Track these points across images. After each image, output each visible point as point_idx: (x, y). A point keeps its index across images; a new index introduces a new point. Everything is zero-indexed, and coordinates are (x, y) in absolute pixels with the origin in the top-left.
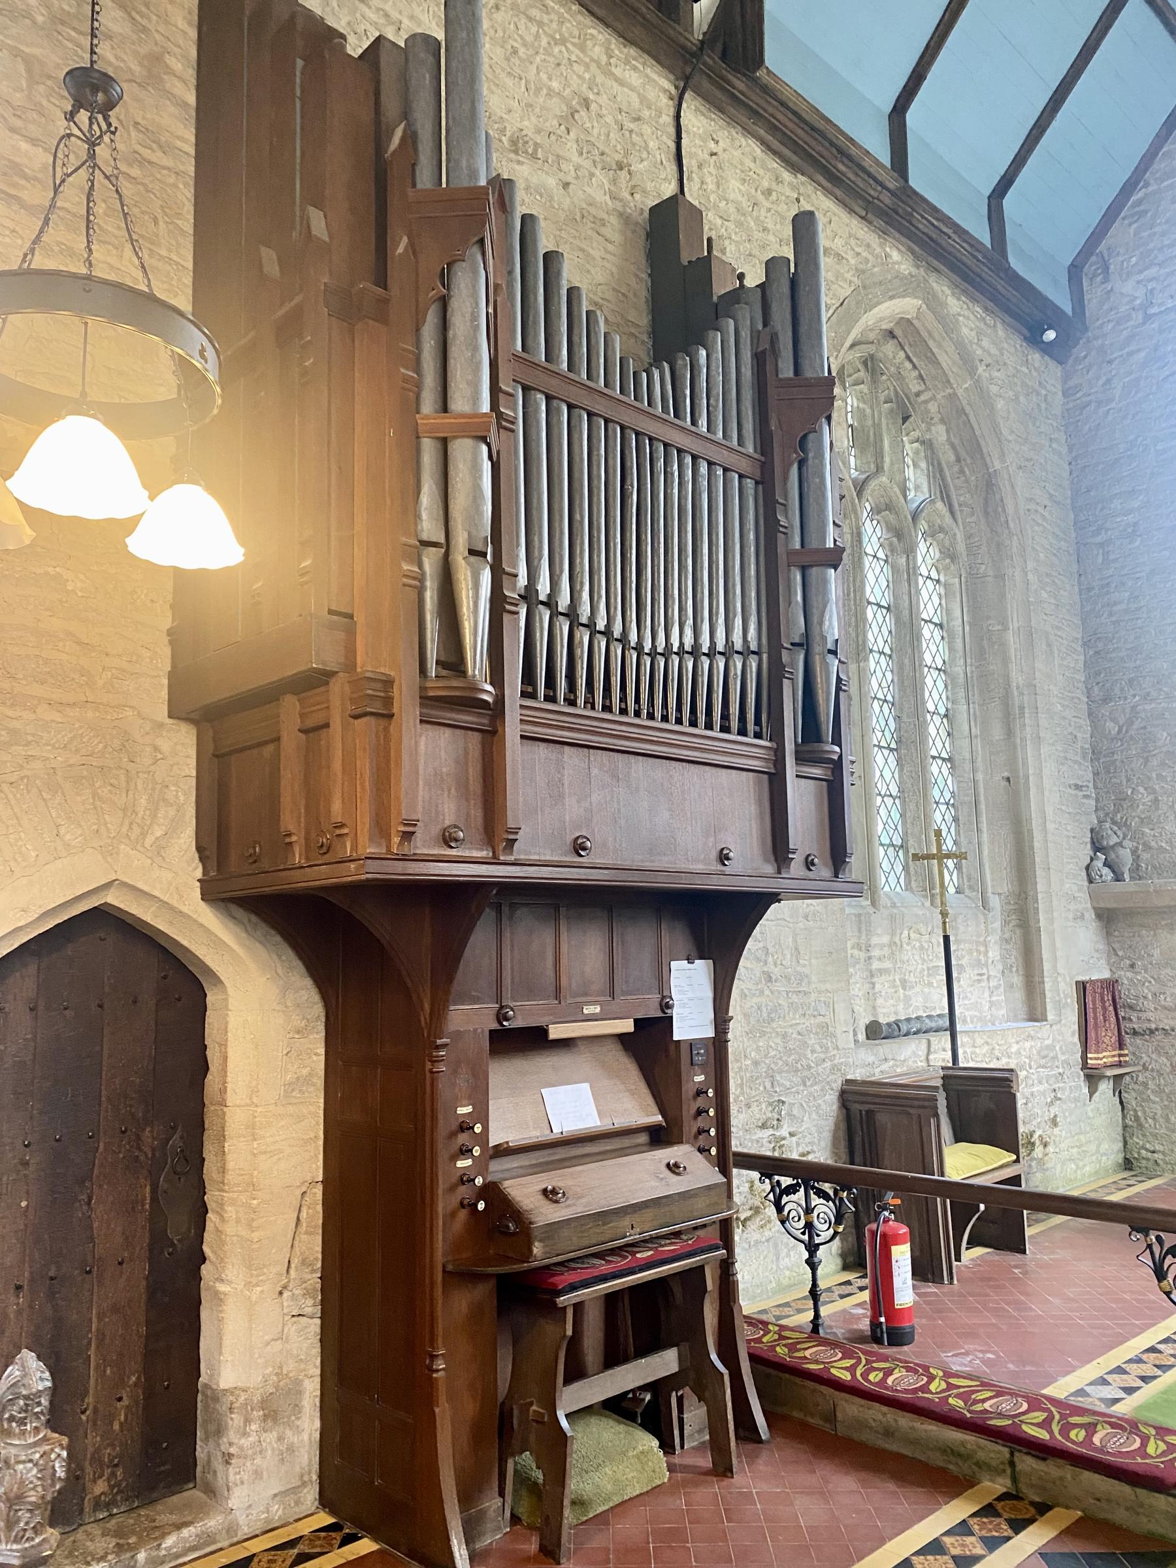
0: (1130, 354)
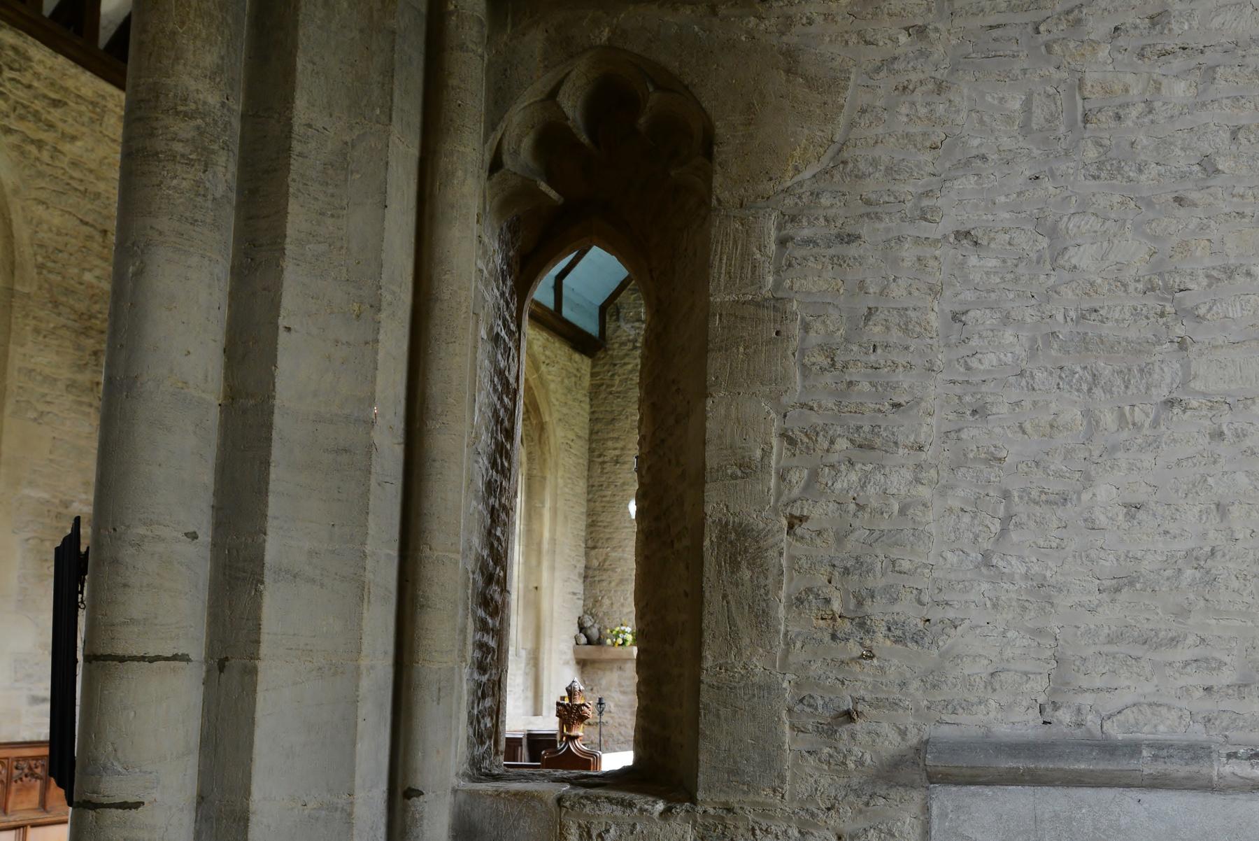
0: (625, 364)
